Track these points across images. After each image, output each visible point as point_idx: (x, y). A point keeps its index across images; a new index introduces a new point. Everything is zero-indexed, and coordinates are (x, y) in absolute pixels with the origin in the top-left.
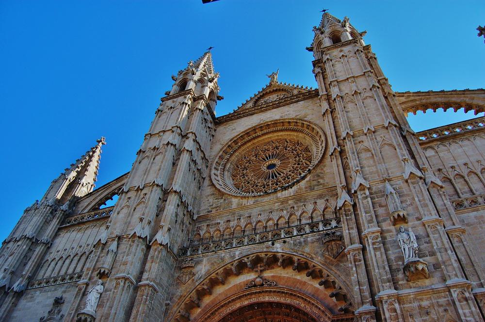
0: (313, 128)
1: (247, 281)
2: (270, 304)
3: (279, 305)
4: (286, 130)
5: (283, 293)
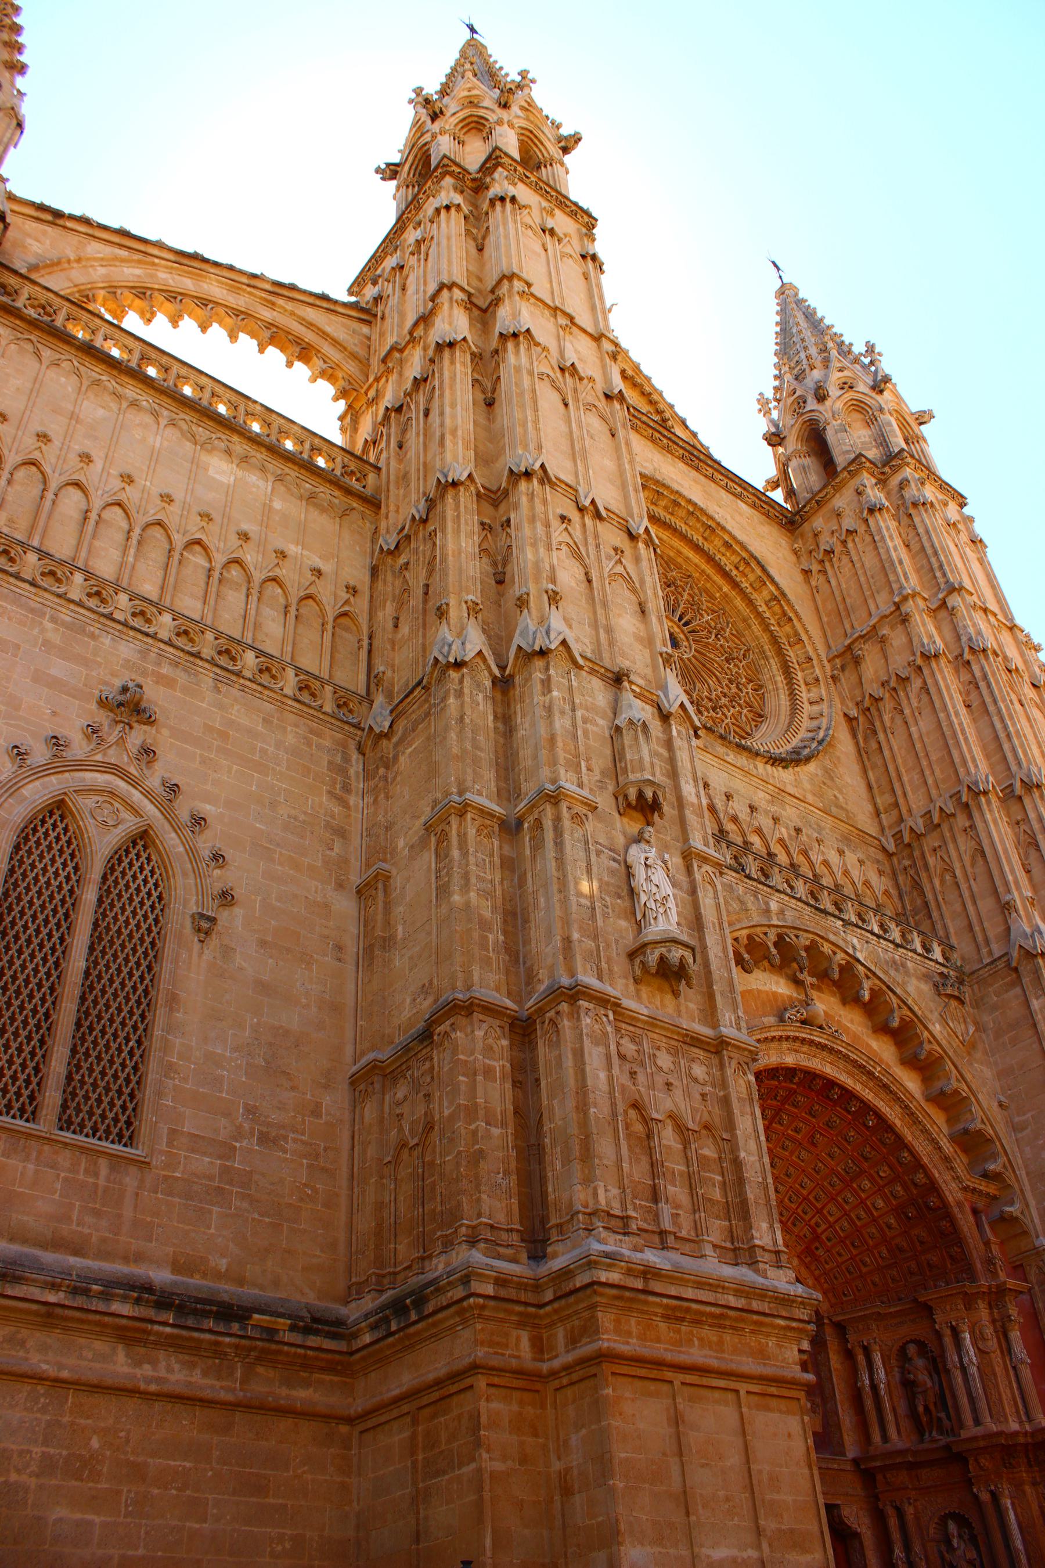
0: (790, 619)
1: (775, 994)
2: (831, 1083)
3: (848, 1095)
4: (710, 559)
5: (870, 1074)
